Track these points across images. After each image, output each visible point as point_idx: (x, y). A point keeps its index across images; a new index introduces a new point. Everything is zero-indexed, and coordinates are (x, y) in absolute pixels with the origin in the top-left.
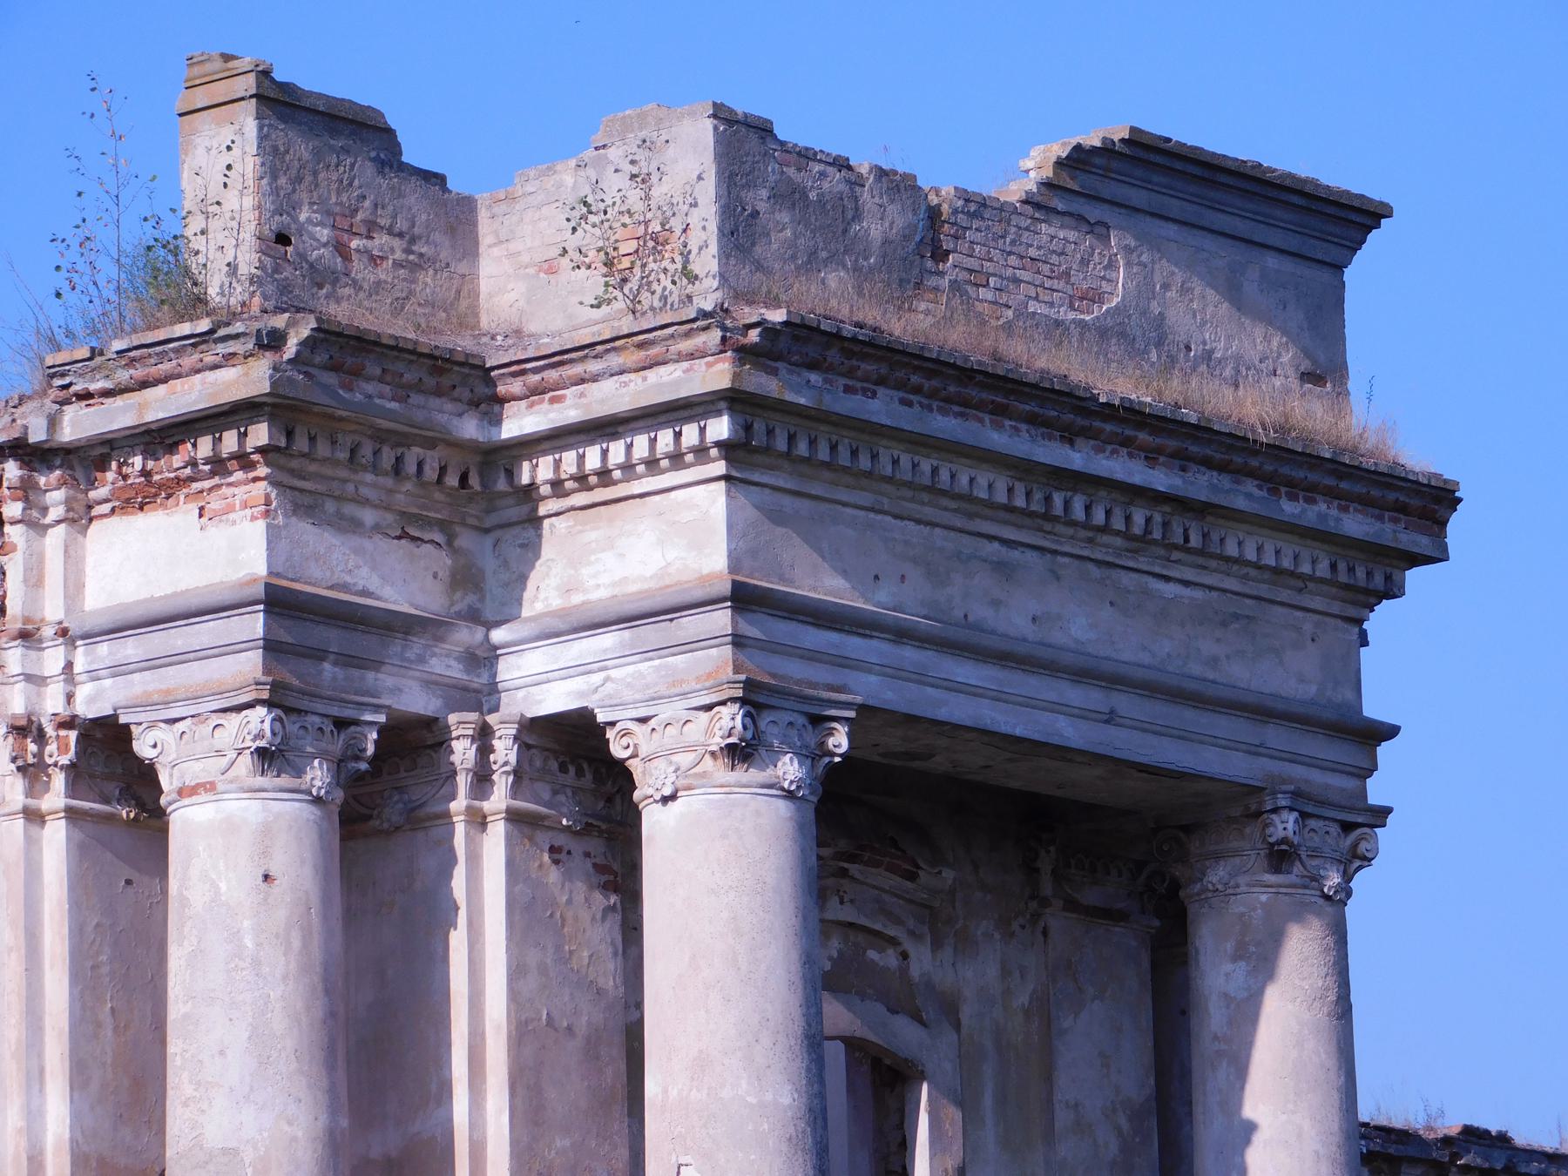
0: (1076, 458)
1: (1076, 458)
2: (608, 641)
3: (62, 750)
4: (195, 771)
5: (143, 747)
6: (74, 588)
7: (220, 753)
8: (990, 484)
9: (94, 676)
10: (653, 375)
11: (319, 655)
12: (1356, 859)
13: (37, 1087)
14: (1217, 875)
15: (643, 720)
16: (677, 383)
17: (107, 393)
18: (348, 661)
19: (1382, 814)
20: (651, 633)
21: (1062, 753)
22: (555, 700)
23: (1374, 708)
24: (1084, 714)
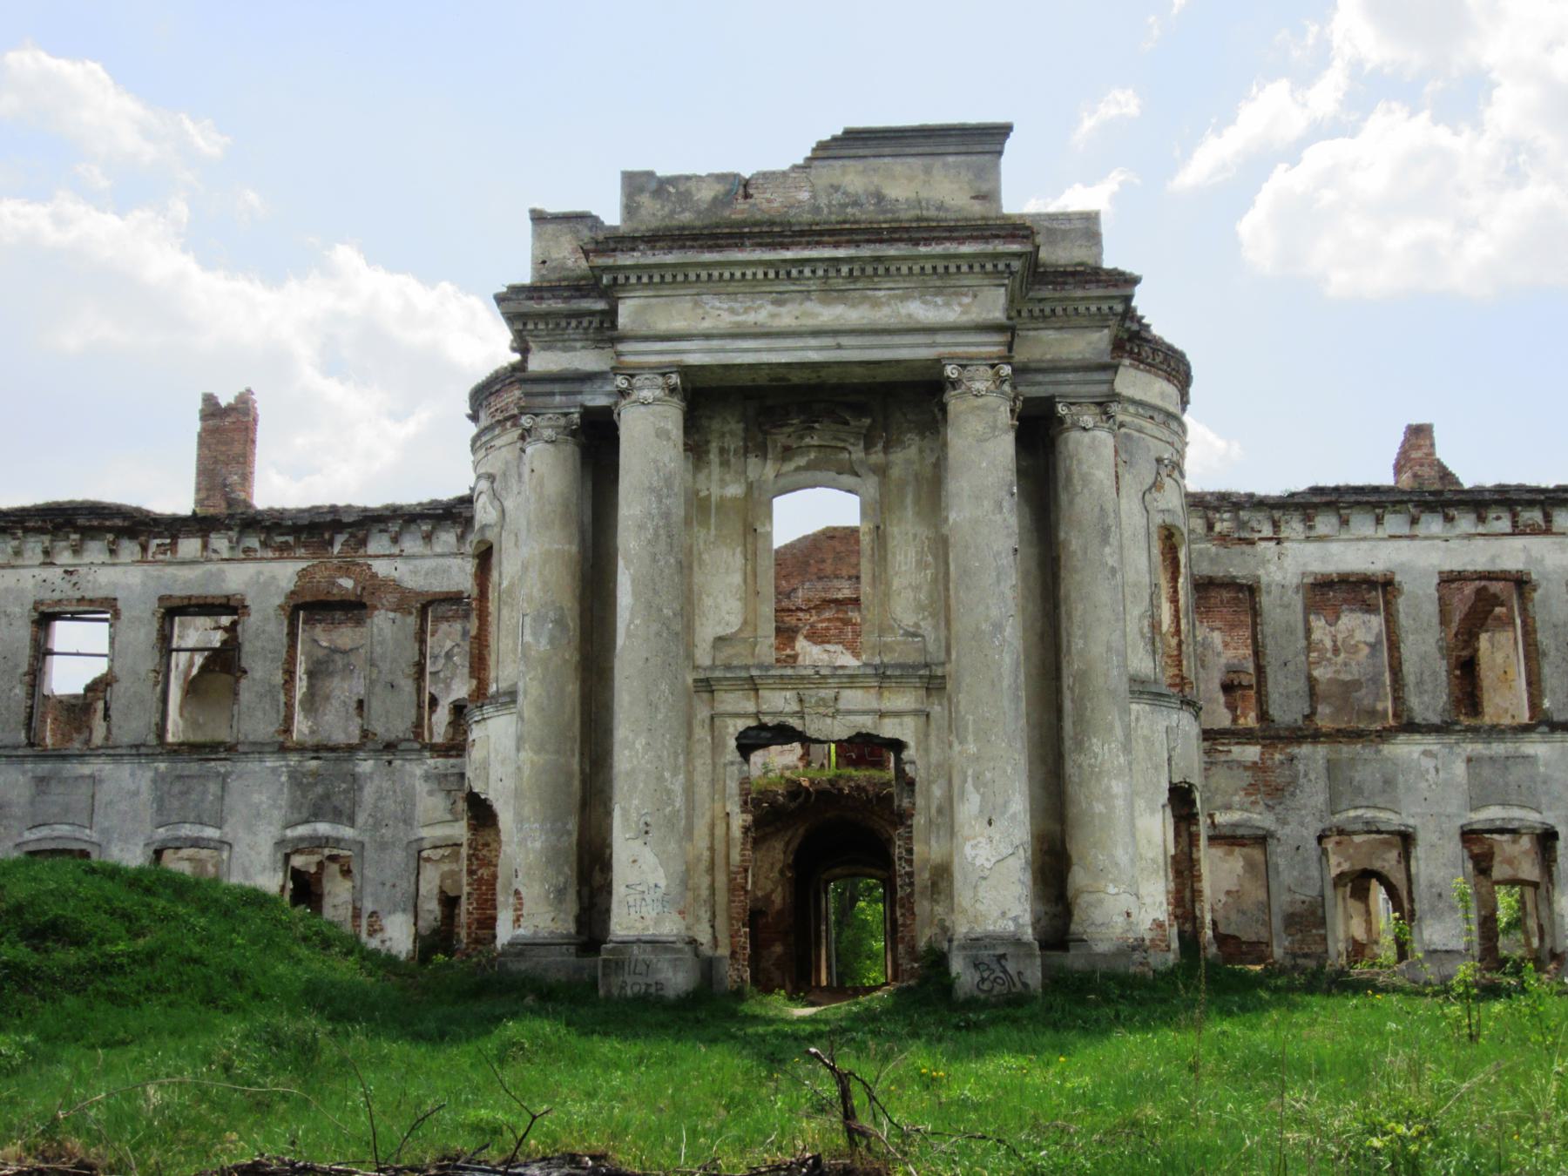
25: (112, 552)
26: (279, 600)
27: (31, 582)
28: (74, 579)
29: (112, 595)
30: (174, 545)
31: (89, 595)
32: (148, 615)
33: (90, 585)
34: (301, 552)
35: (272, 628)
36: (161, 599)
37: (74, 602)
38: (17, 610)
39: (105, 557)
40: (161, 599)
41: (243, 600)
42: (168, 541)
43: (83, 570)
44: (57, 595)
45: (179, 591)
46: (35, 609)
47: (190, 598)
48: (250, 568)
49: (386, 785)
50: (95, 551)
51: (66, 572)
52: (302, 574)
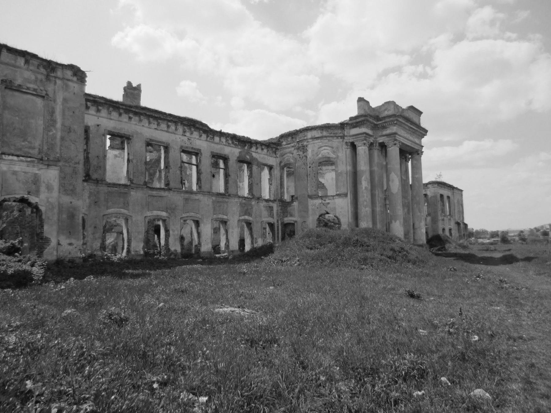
0: (412, 126)
1: (412, 126)
2: (385, 137)
3: (349, 144)
4: (359, 145)
5: (355, 143)
6: (349, 133)
8: (407, 128)
11: (367, 137)
12: (422, 154)
14: (414, 155)
19: (423, 152)
21: (408, 146)
22: (381, 141)
25: (201, 136)
26: (236, 158)
27: (179, 140)
28: (191, 141)
29: (200, 148)
30: (213, 138)
31: (194, 147)
34: (239, 147)
35: (235, 165)
36: (211, 152)
38: (176, 147)
39: (198, 137)
40: (211, 152)
41: (228, 157)
44: (186, 145)
47: (217, 153)
50: (196, 134)
52: (240, 153)
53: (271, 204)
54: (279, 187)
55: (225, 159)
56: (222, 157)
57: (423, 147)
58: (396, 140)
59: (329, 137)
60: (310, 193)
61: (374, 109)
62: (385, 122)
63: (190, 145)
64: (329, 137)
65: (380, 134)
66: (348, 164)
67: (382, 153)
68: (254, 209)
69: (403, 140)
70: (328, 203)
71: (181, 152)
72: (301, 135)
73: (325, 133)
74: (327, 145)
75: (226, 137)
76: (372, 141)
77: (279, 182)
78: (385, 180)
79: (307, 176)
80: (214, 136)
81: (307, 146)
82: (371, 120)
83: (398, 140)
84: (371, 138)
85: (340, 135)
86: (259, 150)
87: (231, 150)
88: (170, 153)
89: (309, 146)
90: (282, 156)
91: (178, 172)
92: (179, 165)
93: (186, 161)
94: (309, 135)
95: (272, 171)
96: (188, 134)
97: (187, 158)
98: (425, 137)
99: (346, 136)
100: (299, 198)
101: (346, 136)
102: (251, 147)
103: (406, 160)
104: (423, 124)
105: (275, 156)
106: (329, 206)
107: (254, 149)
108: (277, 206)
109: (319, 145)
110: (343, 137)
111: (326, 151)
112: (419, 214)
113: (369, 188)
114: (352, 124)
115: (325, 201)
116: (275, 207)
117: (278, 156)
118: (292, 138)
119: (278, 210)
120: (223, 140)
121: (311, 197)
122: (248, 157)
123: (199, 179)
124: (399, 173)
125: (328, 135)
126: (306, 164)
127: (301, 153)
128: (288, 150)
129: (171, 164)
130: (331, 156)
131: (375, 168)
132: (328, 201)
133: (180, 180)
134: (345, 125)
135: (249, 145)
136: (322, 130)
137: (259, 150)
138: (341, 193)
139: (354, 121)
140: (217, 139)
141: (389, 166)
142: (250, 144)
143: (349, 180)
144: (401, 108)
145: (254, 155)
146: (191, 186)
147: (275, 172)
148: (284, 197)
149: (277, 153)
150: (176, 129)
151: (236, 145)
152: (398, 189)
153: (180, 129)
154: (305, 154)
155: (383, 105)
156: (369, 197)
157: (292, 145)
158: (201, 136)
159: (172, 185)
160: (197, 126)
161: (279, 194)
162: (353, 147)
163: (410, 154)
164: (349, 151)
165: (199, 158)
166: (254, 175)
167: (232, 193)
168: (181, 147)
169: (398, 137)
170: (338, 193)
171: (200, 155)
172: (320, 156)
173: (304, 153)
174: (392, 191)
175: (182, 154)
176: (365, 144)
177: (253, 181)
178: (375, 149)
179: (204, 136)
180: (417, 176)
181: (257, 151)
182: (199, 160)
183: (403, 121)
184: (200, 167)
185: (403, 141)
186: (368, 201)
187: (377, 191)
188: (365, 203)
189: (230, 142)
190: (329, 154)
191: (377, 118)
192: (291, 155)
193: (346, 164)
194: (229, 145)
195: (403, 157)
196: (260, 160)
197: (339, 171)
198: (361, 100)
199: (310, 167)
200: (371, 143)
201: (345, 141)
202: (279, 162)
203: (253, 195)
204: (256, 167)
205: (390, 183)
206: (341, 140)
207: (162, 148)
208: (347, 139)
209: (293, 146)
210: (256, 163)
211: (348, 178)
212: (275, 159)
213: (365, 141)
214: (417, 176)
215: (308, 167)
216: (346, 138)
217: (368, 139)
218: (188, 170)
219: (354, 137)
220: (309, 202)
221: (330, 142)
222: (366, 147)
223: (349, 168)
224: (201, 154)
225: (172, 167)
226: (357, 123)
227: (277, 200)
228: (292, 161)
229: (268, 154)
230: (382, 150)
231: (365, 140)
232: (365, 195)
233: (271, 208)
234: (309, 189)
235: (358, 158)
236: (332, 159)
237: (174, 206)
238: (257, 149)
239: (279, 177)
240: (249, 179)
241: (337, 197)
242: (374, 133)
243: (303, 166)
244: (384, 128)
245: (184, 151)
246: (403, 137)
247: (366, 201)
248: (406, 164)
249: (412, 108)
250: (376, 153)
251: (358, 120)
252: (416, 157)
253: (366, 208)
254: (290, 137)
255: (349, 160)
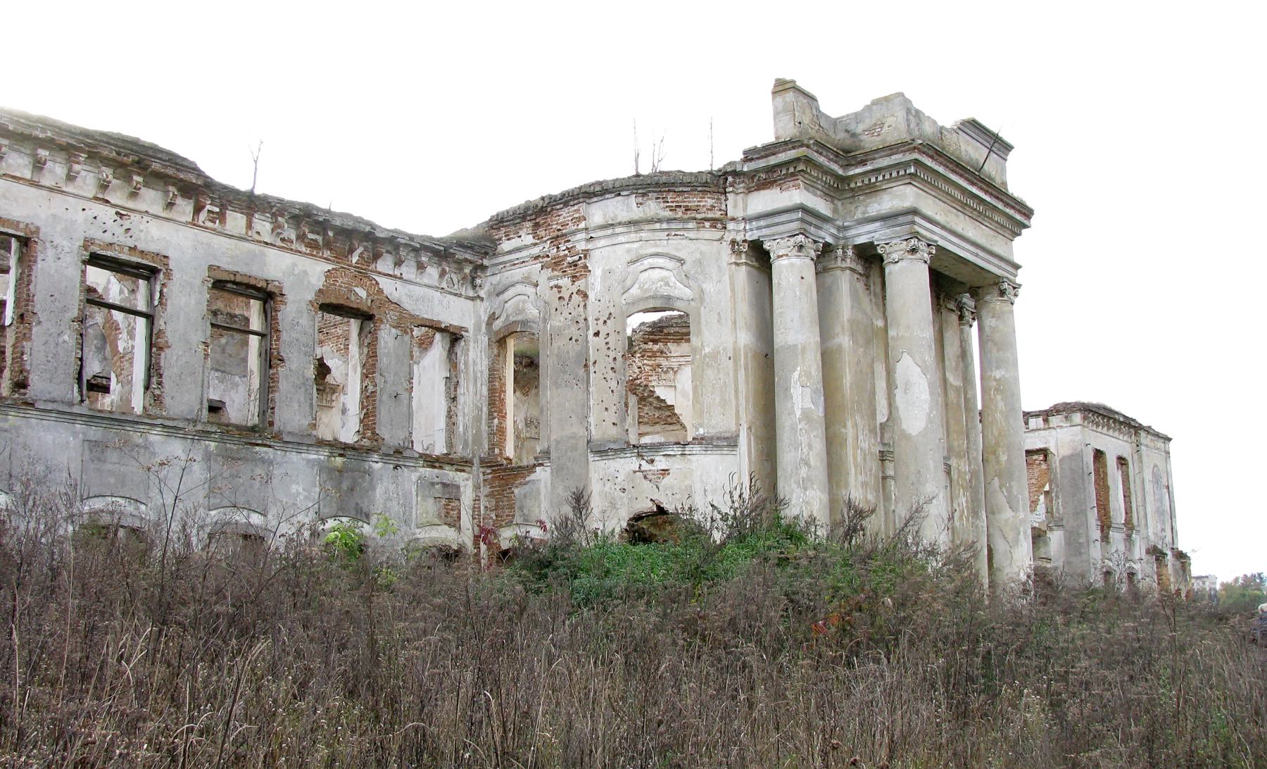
0: (974, 190)
1: (974, 190)
2: (877, 224)
3: (745, 248)
5: (766, 246)
6: (745, 209)
7: (789, 247)
8: (958, 195)
9: (751, 230)
10: (893, 157)
13: (878, 281)
14: (988, 298)
15: (886, 244)
16: (900, 158)
17: (758, 158)
18: (817, 227)
20: (890, 222)
23: (1017, 260)
24: (972, 253)
25: (170, 205)
26: (311, 296)
27: (81, 217)
28: (127, 224)
30: (221, 217)
31: (141, 246)
32: (198, 281)
33: (142, 235)
34: (327, 254)
35: (304, 321)
36: (211, 268)
37: (126, 249)
39: (157, 209)
40: (211, 268)
42: (217, 210)
43: (135, 217)
44: (108, 238)
45: (227, 264)
46: (85, 247)
48: (288, 258)
49: (392, 487)
50: (151, 199)
51: (117, 213)
53: (450, 474)
54: (485, 409)
55: (268, 296)
56: (254, 287)
57: (1017, 267)
58: (916, 235)
59: (669, 220)
60: (596, 434)
61: (835, 122)
62: (877, 171)
63: (122, 239)
64: (669, 220)
65: (859, 215)
66: (741, 323)
67: (867, 287)
68: (379, 491)
69: (942, 237)
70: (665, 472)
71: (85, 263)
72: (565, 214)
73: (653, 207)
74: (660, 250)
75: (274, 215)
76: (829, 240)
77: (485, 391)
78: (881, 385)
79: (586, 366)
80: (223, 208)
81: (586, 253)
82: (822, 160)
83: (923, 237)
84: (826, 226)
85: (710, 215)
86: (408, 271)
87: (295, 265)
88: (40, 264)
89: (596, 255)
90: (498, 295)
91: (69, 338)
92: (75, 313)
93: (117, 303)
94: (598, 212)
95: (459, 349)
96: (117, 197)
97: (121, 292)
98: (1024, 231)
99: (733, 219)
100: (553, 455)
101: (733, 219)
102: (376, 257)
103: (961, 317)
104: (1014, 189)
105: (471, 293)
106: (667, 481)
107: (385, 264)
108: (477, 487)
109: (629, 251)
110: (719, 223)
111: (656, 274)
112: (1008, 514)
113: (820, 412)
114: (752, 175)
115: (652, 461)
116: (467, 485)
117: (482, 293)
118: (537, 225)
119: (477, 499)
120: (263, 225)
121: (602, 451)
122: (362, 293)
123: (153, 370)
124: (930, 357)
125: (668, 213)
126: (582, 325)
127: (565, 282)
128: (517, 273)
129: (40, 303)
130: (675, 293)
131: (844, 340)
132: (661, 463)
133: (73, 369)
134: (730, 179)
135: (366, 249)
136: (644, 195)
137: (408, 271)
138: (713, 432)
139: (762, 163)
140: (236, 221)
141: (892, 333)
142: (369, 244)
143: (743, 384)
144: (934, 122)
145: (386, 285)
146: (126, 400)
147: (472, 354)
148: (502, 449)
149: (478, 281)
150: (71, 178)
151: (313, 245)
152: (930, 421)
153: (88, 179)
154: (580, 284)
155: (868, 108)
156: (819, 445)
157: (536, 251)
158: (170, 205)
159: (38, 385)
160: (156, 166)
161: (485, 435)
162: (760, 256)
163: (975, 292)
164: (744, 275)
165: (158, 288)
166: (383, 361)
167: (289, 429)
168: (88, 242)
169: (922, 226)
170: (701, 431)
171: (161, 275)
172: (635, 291)
173: (574, 278)
174: (904, 426)
175: (91, 270)
176: (801, 247)
177: (381, 385)
178: (843, 269)
179: (185, 207)
180: (998, 374)
181: (397, 273)
182: (157, 295)
183: (941, 169)
184: (160, 323)
185: (942, 243)
186: (812, 463)
187: (849, 424)
188: (804, 471)
189: (291, 234)
190: (667, 284)
191: (848, 155)
192: (530, 290)
193: (735, 322)
194: (285, 245)
195: (952, 305)
196: (408, 305)
197: (707, 350)
198: (783, 87)
199: (597, 334)
200: (827, 246)
201: (729, 237)
202: (485, 318)
203: (375, 437)
204: (394, 331)
205: (899, 393)
206: (718, 234)
207: (14, 244)
208: (737, 231)
209: (537, 258)
210: (393, 315)
211: (742, 373)
212: (470, 303)
213: (801, 238)
214: (998, 374)
215: (591, 332)
216: (731, 226)
217: (812, 229)
218: (124, 336)
219: (762, 223)
220: (592, 466)
221: (674, 242)
222: (808, 261)
223: (745, 338)
224: (168, 275)
225: (42, 316)
226: (771, 169)
227: (476, 461)
228: (532, 312)
229: (444, 285)
230: (867, 277)
231: (804, 233)
232: (803, 439)
233: (450, 494)
234: (591, 419)
235: (776, 298)
236: (678, 304)
237: (40, 468)
238: (398, 263)
239: (486, 373)
240: (365, 376)
241: (697, 448)
242: (835, 211)
243: (573, 331)
244: (872, 190)
245: (96, 260)
246: (944, 228)
247: (807, 464)
248: (962, 332)
249: (974, 127)
250: (845, 282)
251: (773, 160)
252: (994, 302)
253: (806, 489)
254: (529, 224)
255: (744, 308)
